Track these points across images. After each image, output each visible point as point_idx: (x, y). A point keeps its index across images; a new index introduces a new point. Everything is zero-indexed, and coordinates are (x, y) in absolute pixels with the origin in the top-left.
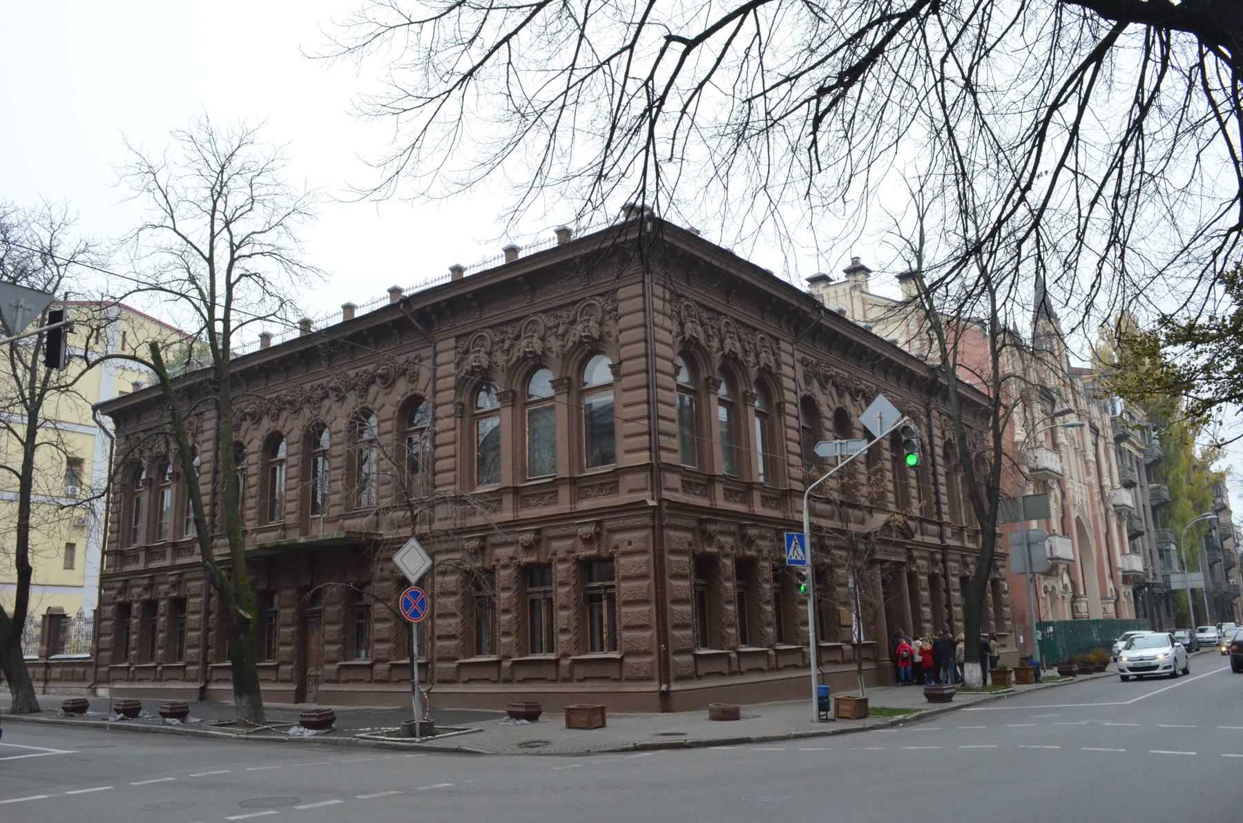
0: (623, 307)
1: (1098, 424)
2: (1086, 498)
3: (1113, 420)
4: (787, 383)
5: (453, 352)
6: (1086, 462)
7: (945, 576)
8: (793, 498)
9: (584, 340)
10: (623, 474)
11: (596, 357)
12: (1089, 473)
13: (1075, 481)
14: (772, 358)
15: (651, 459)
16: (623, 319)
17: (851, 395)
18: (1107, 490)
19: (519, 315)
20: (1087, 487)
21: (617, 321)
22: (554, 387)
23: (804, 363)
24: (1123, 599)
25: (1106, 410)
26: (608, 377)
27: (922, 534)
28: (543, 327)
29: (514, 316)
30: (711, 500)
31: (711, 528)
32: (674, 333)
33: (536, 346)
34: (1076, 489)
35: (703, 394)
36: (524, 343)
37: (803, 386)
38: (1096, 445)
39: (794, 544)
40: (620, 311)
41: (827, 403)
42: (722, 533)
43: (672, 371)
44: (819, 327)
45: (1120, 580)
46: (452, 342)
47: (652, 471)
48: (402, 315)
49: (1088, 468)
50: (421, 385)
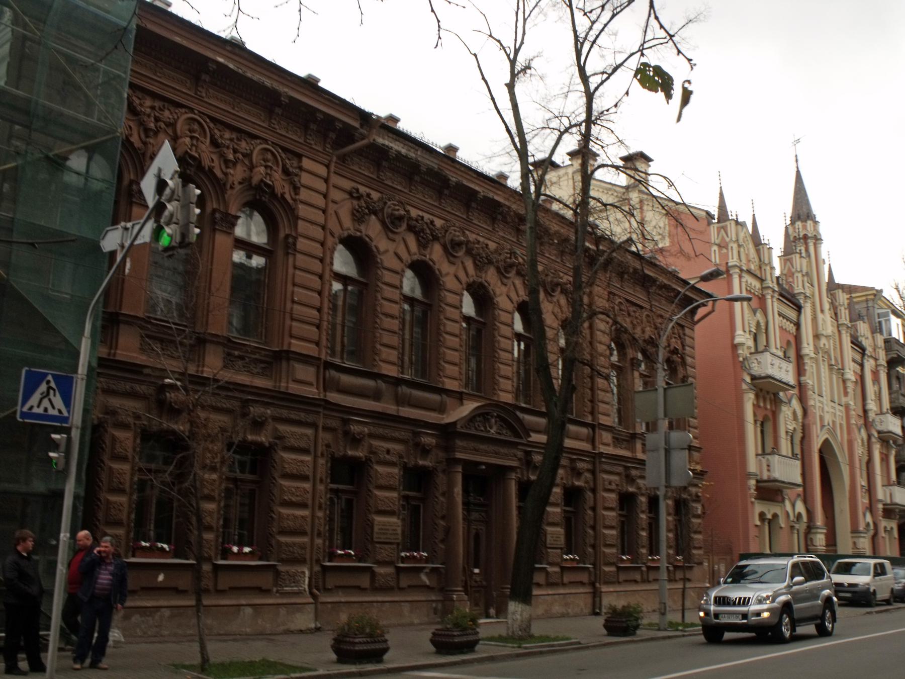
1: (867, 343)
2: (840, 419)
3: (887, 341)
6: (844, 381)
7: (594, 491)
13: (826, 399)
18: (871, 415)
20: (842, 409)
23: (353, 194)
24: (882, 533)
25: (881, 332)
30: (111, 348)
34: (826, 408)
39: (43, 387)
45: (880, 513)
49: (845, 388)
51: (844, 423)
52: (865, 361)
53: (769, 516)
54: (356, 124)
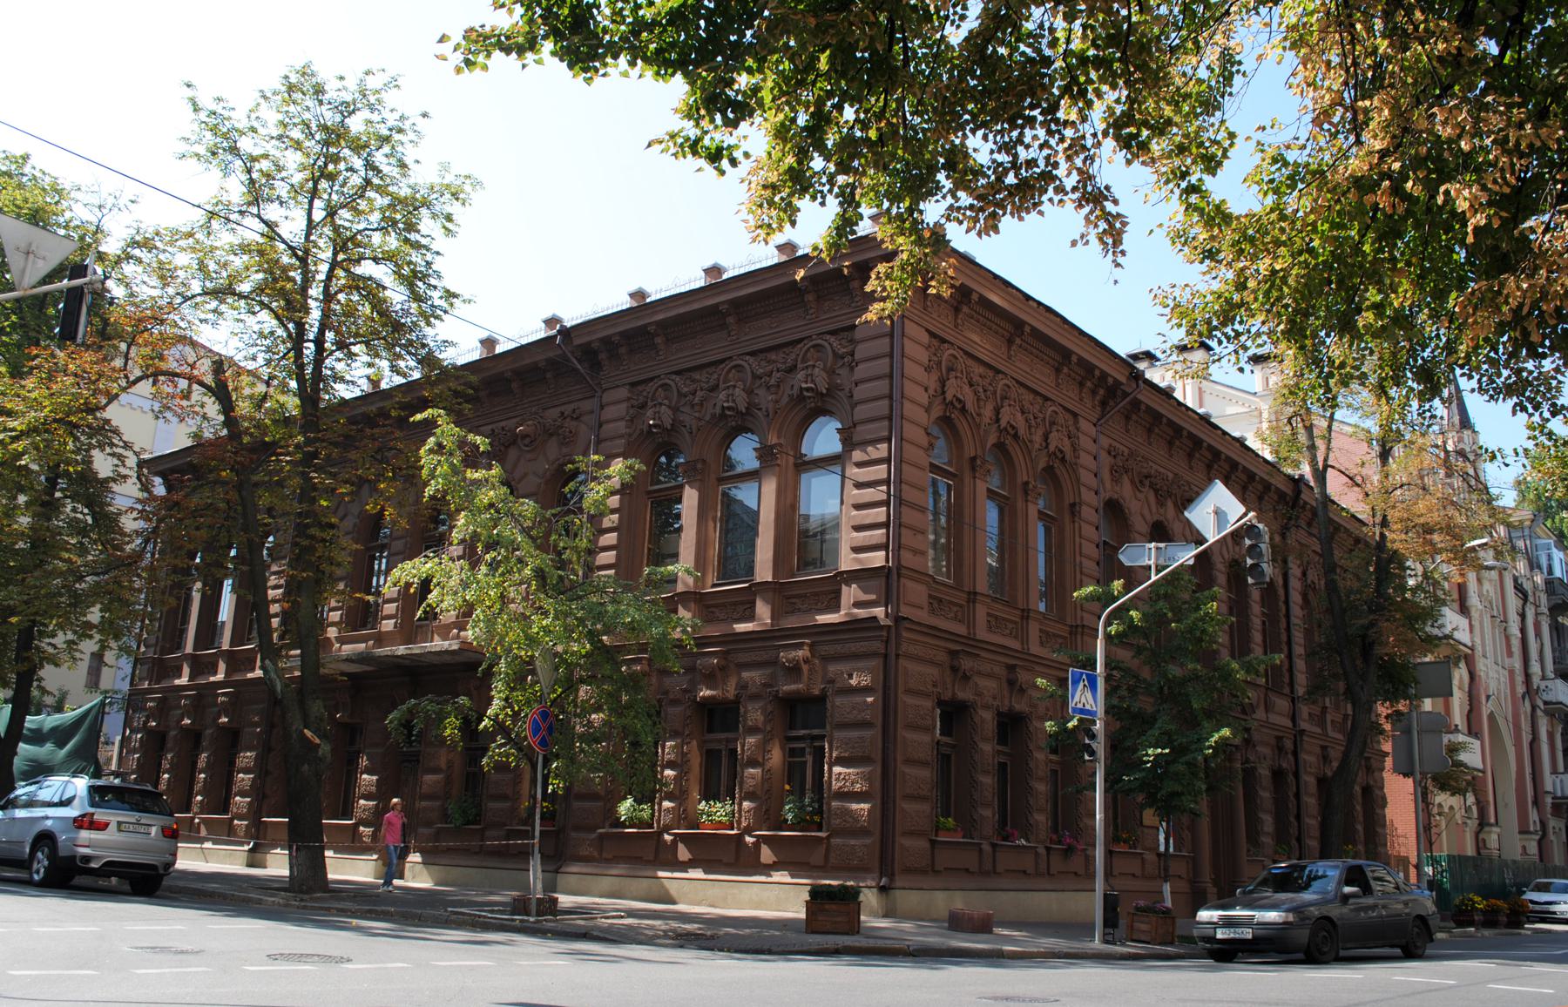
0: (861, 351)
1: (1527, 586)
2: (1505, 689)
4: (1086, 477)
5: (624, 406)
7: (1296, 775)
8: (1085, 638)
9: (806, 394)
11: (821, 419)
12: (1510, 654)
13: (1490, 662)
14: (1066, 441)
15: (887, 561)
16: (861, 366)
17: (1175, 505)
18: (1536, 681)
19: (719, 357)
20: (1506, 673)
21: (852, 369)
22: (759, 458)
25: (1539, 567)
26: (836, 447)
27: (1267, 710)
28: (749, 374)
29: (713, 359)
31: (966, 664)
32: (931, 391)
33: (738, 400)
34: (1491, 674)
35: (967, 479)
37: (1108, 485)
38: (1523, 616)
40: (857, 356)
41: (1139, 507)
42: (979, 673)
43: (925, 444)
44: (1136, 404)
45: (1549, 809)
46: (623, 393)
47: (888, 577)
48: (560, 352)
51: (1508, 691)
52: (1527, 609)
53: (1446, 810)
54: (1123, 380)
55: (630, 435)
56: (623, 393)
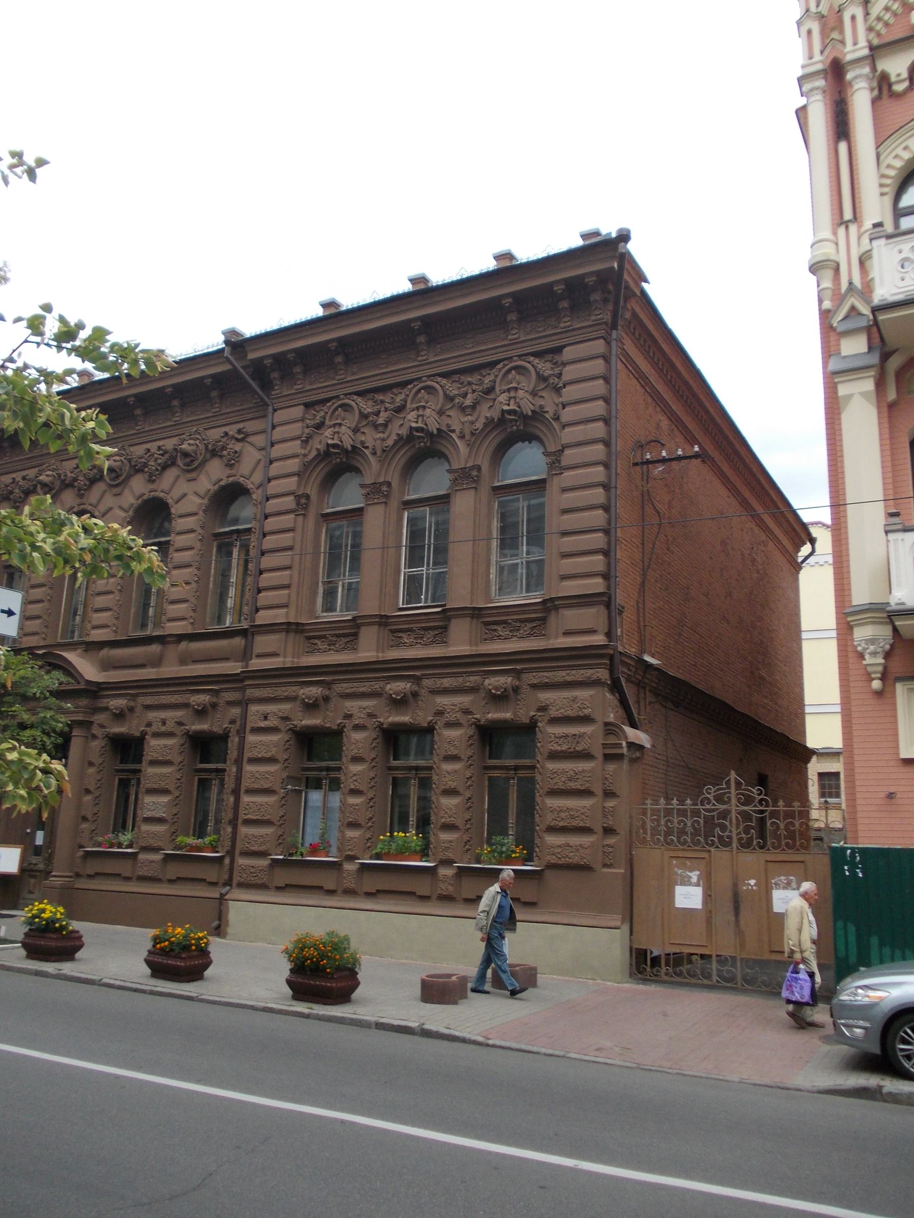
10: (557, 608)
33: (429, 421)
36: (412, 415)
40: (566, 377)
46: (298, 411)
48: (226, 367)
50: (245, 467)
55: (305, 455)
56: (298, 411)
